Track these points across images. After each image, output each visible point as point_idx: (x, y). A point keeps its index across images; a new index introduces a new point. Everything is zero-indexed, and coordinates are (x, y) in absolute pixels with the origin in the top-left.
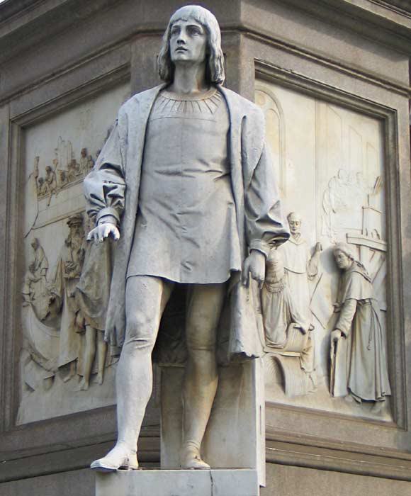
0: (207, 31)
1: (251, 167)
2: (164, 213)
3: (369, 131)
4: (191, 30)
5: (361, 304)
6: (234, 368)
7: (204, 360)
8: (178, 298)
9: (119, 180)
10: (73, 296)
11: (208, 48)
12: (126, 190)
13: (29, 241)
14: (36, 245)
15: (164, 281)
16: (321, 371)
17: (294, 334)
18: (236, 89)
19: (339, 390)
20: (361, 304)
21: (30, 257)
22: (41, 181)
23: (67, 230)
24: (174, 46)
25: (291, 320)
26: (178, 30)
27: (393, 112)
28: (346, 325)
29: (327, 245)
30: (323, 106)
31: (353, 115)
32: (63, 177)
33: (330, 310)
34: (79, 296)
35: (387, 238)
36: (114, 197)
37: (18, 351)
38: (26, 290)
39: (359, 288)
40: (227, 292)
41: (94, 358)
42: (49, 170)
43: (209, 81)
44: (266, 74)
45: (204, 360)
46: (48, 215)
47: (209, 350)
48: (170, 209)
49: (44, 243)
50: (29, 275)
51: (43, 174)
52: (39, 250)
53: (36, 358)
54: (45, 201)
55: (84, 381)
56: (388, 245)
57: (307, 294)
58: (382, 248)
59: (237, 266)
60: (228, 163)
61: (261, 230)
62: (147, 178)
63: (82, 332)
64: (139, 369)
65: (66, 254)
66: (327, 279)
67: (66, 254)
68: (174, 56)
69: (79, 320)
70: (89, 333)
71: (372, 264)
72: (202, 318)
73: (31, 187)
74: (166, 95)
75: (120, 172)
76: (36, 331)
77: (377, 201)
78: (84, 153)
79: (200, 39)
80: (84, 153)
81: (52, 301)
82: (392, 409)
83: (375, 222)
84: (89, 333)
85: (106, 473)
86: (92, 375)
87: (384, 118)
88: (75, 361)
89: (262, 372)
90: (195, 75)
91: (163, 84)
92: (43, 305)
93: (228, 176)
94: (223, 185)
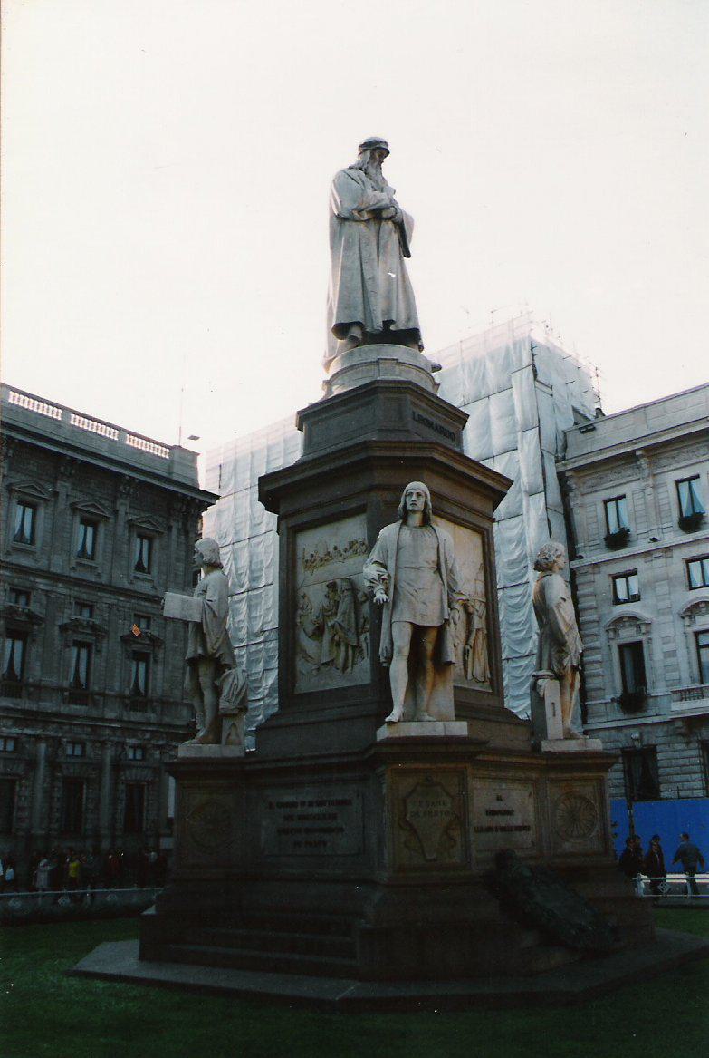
0: (426, 496)
1: (450, 566)
5: (478, 630)
6: (442, 666)
7: (429, 665)
8: (418, 632)
9: (383, 570)
10: (333, 626)
12: (389, 576)
15: (411, 623)
19: (470, 677)
21: (301, 602)
22: (307, 561)
23: (326, 589)
30: (457, 527)
31: (470, 531)
32: (322, 560)
34: (337, 627)
36: (383, 579)
37: (294, 654)
38: (298, 620)
42: (312, 556)
45: (429, 665)
46: (311, 579)
47: (431, 660)
48: (413, 586)
50: (299, 612)
51: (308, 558)
52: (306, 598)
53: (307, 657)
54: (308, 573)
55: (339, 671)
56: (487, 599)
58: (484, 601)
59: (447, 617)
60: (439, 564)
63: (338, 645)
64: (399, 672)
65: (326, 602)
67: (326, 602)
69: (336, 638)
73: (300, 564)
74: (405, 528)
75: (385, 566)
76: (308, 644)
77: (481, 577)
79: (422, 500)
80: (335, 548)
83: (480, 587)
86: (345, 668)
88: (333, 660)
91: (401, 521)
92: (310, 628)
93: (439, 570)
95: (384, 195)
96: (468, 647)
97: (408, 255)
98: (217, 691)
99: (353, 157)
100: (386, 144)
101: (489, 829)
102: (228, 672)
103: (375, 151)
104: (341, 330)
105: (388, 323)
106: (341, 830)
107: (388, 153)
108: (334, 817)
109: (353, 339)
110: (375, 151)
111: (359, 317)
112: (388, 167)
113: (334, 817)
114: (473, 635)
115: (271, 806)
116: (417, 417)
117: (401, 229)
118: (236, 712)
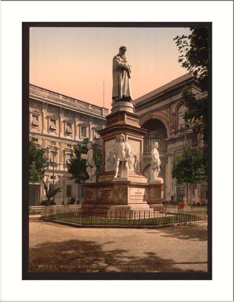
3: (139, 143)
6: (125, 168)
8: (121, 162)
11: (123, 138)
18: (126, 142)
20: (138, 160)
25: (131, 162)
27: (141, 140)
33: (135, 161)
43: (123, 141)
44: (129, 138)
57: (132, 160)
61: (127, 156)
63: (111, 163)
66: (134, 159)
71: (139, 156)
72: (123, 163)
75: (115, 150)
81: (108, 160)
89: (128, 168)
90: (122, 141)
94: (125, 152)
95: (124, 63)
97: (129, 77)
99: (118, 52)
100: (126, 48)
101: (135, 196)
103: (123, 50)
104: (113, 98)
105: (123, 96)
106: (110, 195)
107: (126, 50)
109: (116, 100)
110: (123, 50)
111: (117, 95)
112: (127, 54)
117: (128, 71)
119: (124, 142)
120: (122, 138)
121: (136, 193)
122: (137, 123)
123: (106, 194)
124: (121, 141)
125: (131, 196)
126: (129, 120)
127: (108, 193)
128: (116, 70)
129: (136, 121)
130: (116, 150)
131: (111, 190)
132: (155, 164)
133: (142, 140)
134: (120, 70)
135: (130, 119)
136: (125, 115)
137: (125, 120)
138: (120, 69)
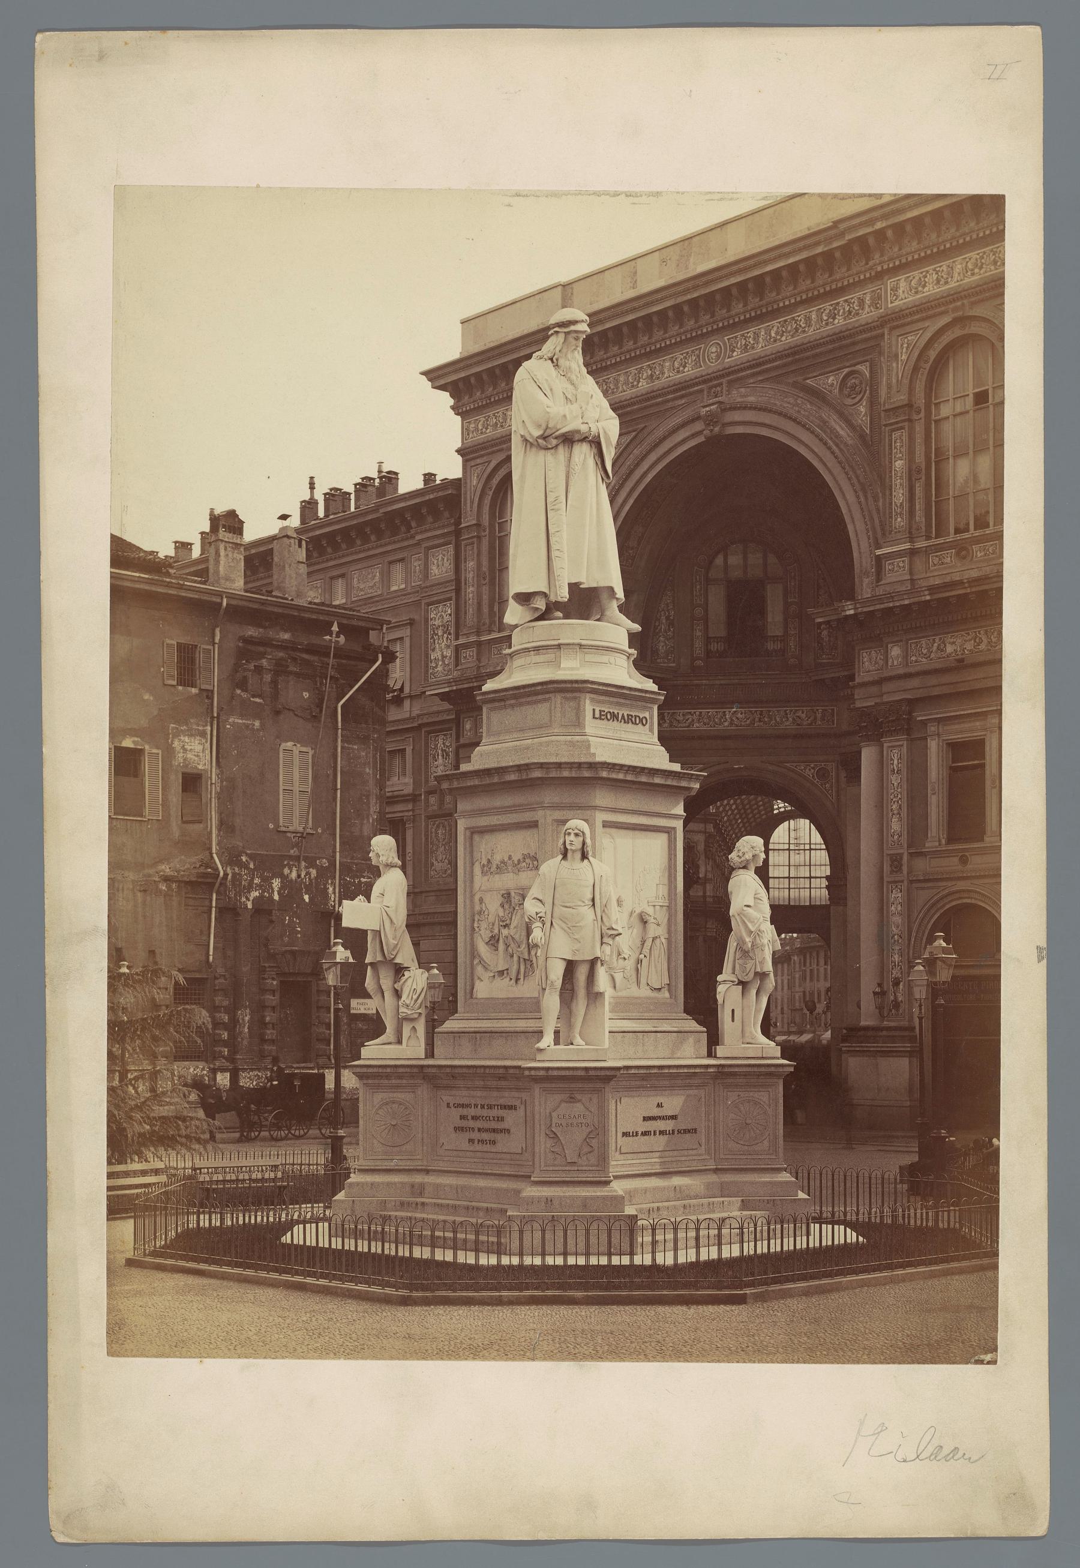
2: (564, 925)
4: (577, 835)
7: (581, 992)
8: (571, 966)
11: (584, 843)
13: (477, 898)
14: (481, 900)
16: (634, 976)
17: (621, 961)
20: (654, 939)
21: (477, 908)
24: (568, 842)
26: (569, 834)
27: (674, 828)
28: (646, 951)
29: (638, 911)
32: (498, 867)
35: (670, 900)
38: (476, 925)
39: (653, 930)
40: (593, 963)
41: (518, 972)
42: (489, 861)
45: (581, 992)
49: (487, 900)
51: (484, 862)
54: (486, 878)
55: (513, 981)
56: (670, 903)
60: (593, 900)
62: (556, 908)
63: (512, 956)
68: (568, 847)
70: (515, 958)
72: (581, 974)
78: (510, 858)
80: (510, 858)
82: (669, 991)
84: (515, 958)
85: (540, 1050)
86: (517, 980)
87: (670, 831)
90: (579, 855)
96: (642, 956)
98: (398, 994)
101: (645, 1133)
102: (406, 973)
106: (508, 1131)
108: (502, 1119)
113: (501, 1119)
114: (648, 943)
115: (448, 1105)
116: (597, 715)
118: (416, 1016)
119: (586, 861)
120: (577, 843)
121: (645, 1119)
122: (651, 730)
123: (494, 1125)
124: (569, 855)
125: (625, 1134)
126: (605, 721)
127: (501, 1119)
128: (532, 444)
129: (642, 721)
130: (548, 901)
131: (518, 1103)
132: (745, 953)
133: (679, 825)
134: (557, 446)
135: (614, 717)
136: (588, 702)
137: (588, 730)
138: (554, 442)
